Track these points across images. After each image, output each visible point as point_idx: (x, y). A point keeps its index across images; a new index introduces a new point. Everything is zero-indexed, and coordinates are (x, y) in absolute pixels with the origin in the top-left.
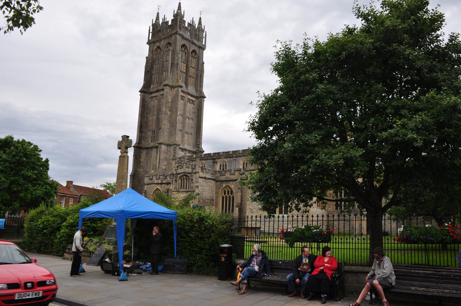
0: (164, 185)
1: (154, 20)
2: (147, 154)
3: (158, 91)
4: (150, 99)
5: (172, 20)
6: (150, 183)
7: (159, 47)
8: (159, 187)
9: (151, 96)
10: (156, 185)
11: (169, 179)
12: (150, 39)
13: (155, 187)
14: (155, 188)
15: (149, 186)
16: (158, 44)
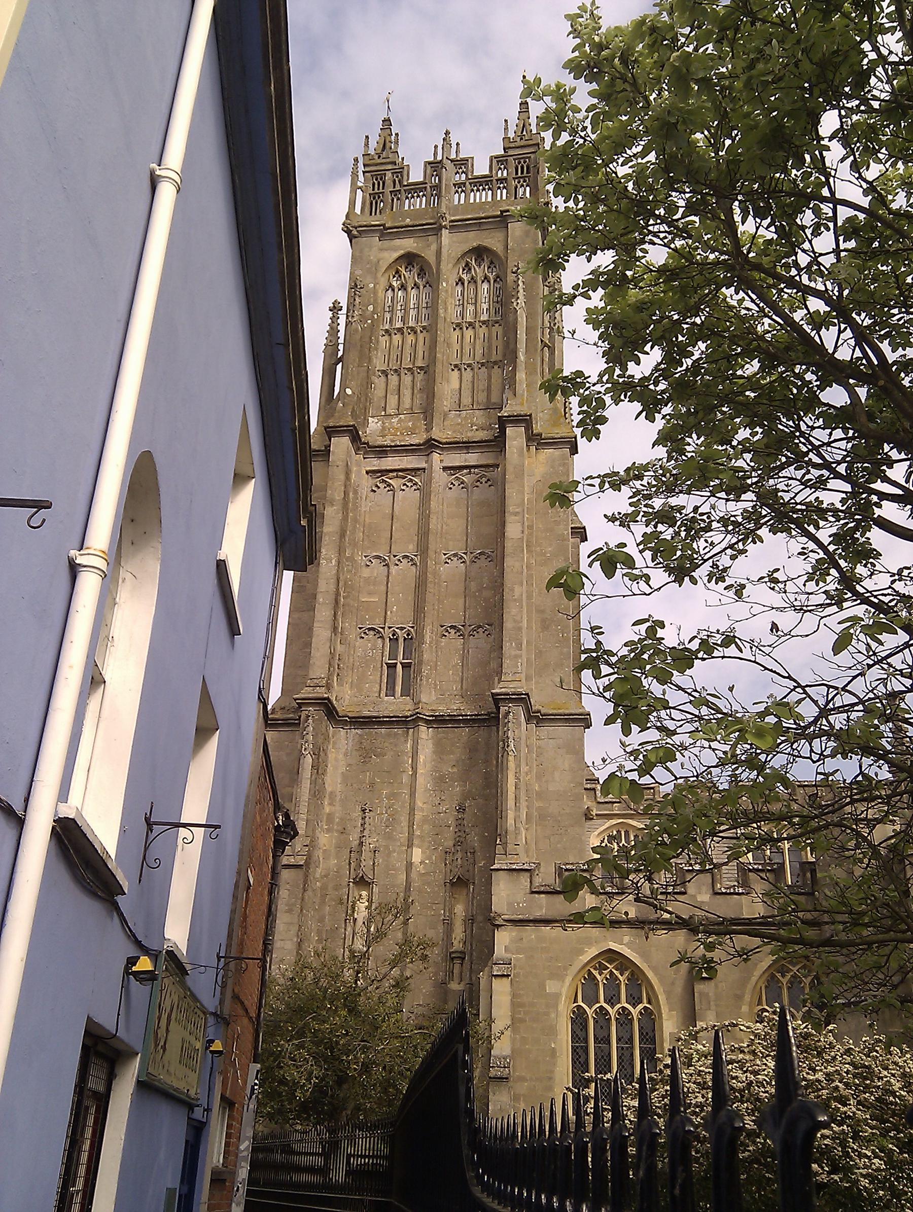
0: (662, 936)
1: (373, 144)
2: (365, 754)
3: (430, 446)
4: (367, 483)
5: (499, 161)
6: (538, 914)
7: (409, 259)
8: (623, 943)
9: (376, 464)
10: (595, 932)
11: (704, 897)
12: (358, 210)
13: (589, 942)
14: (593, 952)
15: (530, 932)
16: (408, 244)
